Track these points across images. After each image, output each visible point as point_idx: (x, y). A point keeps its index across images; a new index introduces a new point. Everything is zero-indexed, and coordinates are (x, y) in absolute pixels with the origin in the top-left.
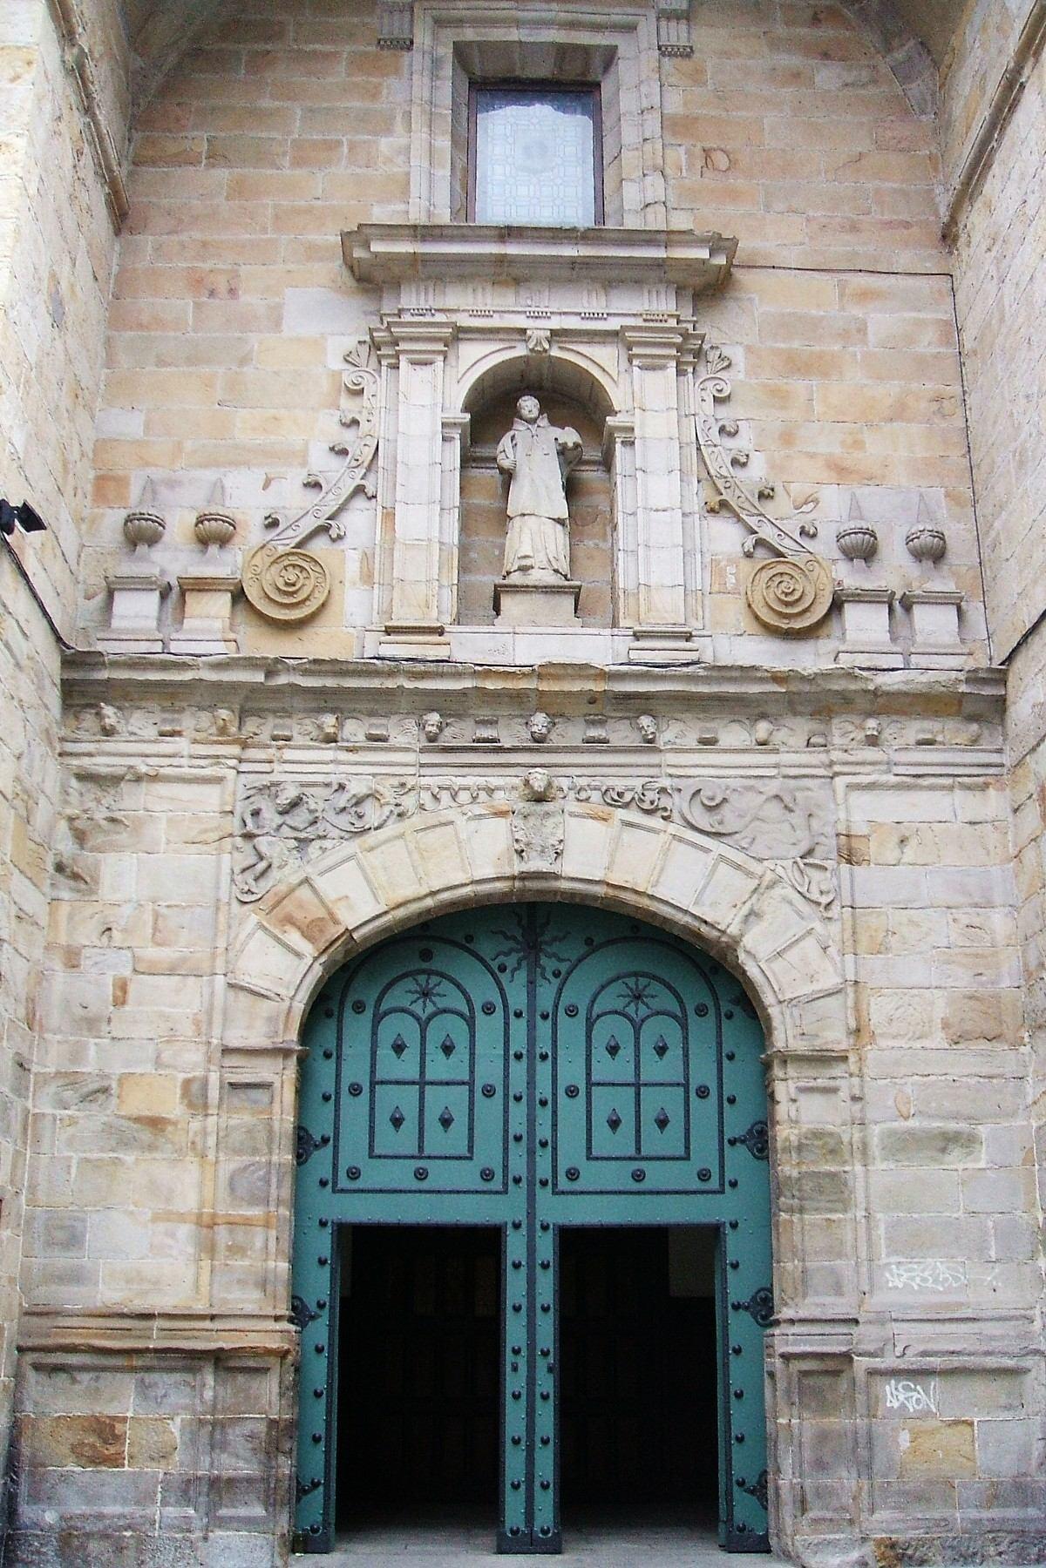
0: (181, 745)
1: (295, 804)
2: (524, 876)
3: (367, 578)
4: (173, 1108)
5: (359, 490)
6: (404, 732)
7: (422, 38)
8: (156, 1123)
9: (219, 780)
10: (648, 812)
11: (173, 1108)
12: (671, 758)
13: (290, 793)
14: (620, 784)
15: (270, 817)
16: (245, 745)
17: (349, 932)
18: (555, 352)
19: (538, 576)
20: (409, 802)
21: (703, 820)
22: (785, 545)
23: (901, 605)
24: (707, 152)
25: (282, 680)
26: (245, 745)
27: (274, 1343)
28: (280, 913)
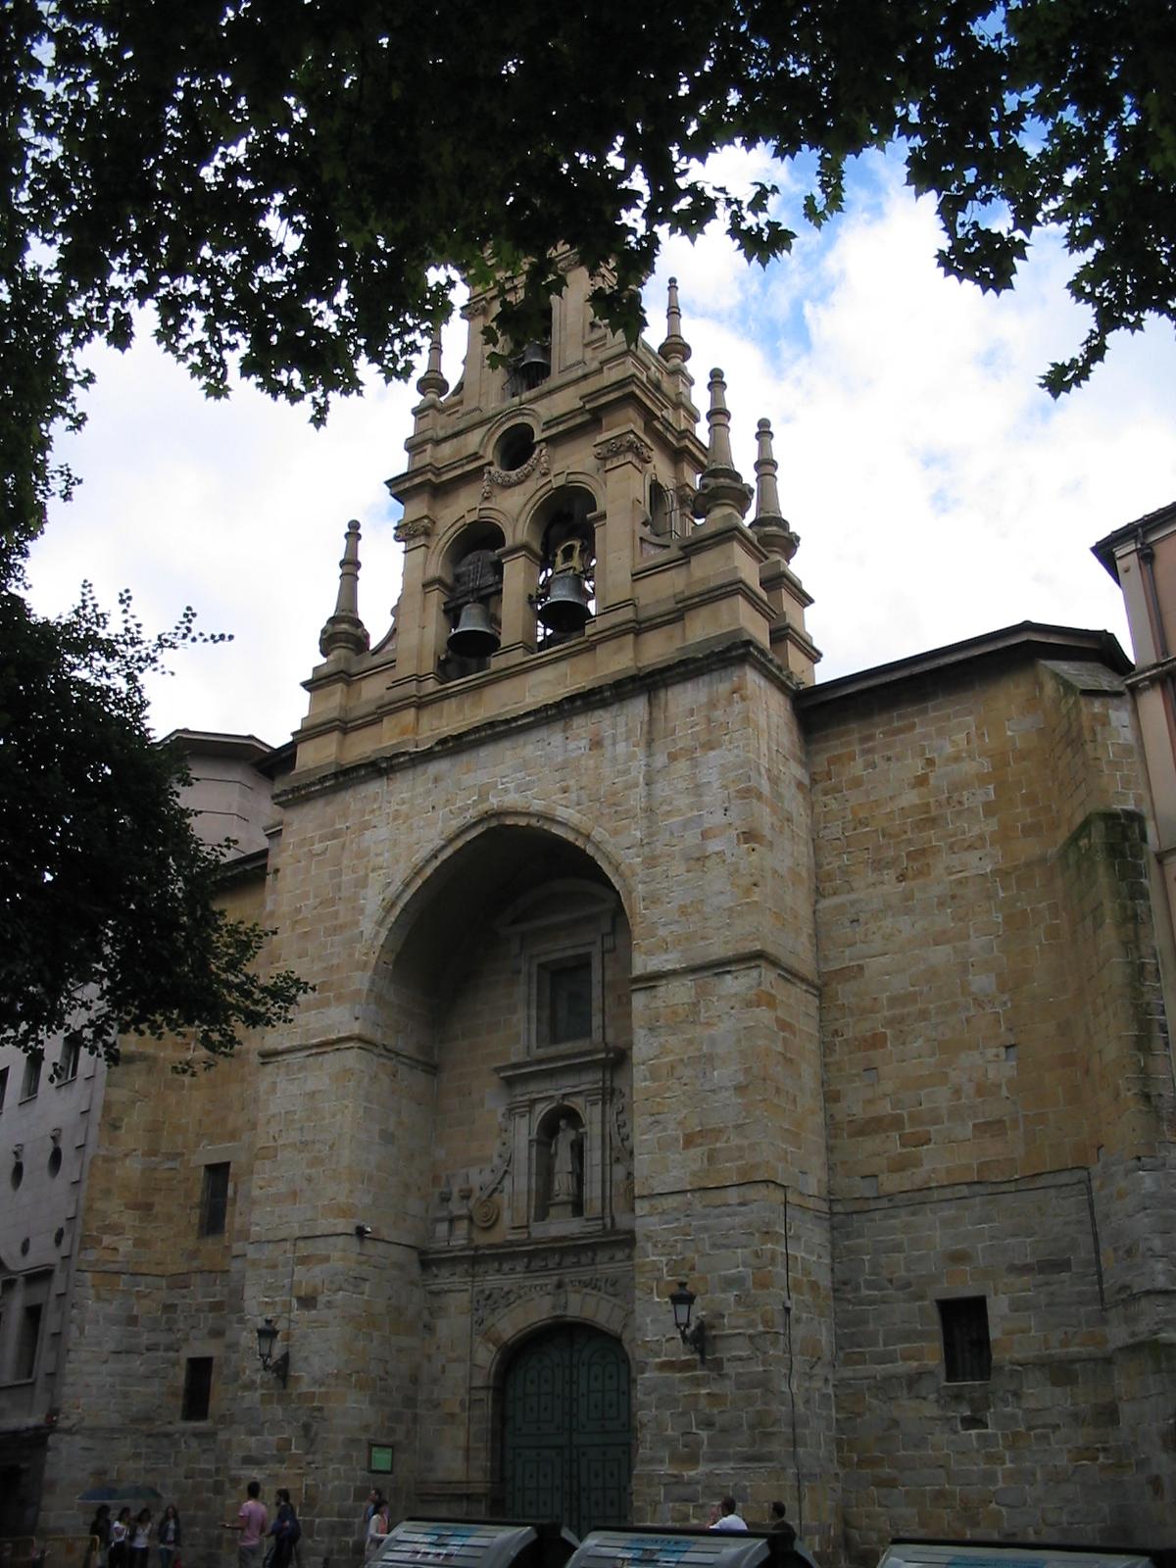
0: (455, 1279)
1: (490, 1296)
2: (557, 1317)
4: (457, 1410)
5: (506, 1172)
6: (520, 1266)
7: (524, 969)
8: (452, 1415)
9: (467, 1290)
10: (593, 1289)
11: (457, 1410)
12: (599, 1267)
13: (487, 1292)
14: (584, 1278)
15: (482, 1302)
16: (473, 1276)
17: (505, 1343)
18: (566, 1103)
20: (522, 1292)
21: (611, 1290)
24: (619, 997)
25: (481, 1252)
26: (473, 1276)
27: (481, 1491)
28: (487, 1336)
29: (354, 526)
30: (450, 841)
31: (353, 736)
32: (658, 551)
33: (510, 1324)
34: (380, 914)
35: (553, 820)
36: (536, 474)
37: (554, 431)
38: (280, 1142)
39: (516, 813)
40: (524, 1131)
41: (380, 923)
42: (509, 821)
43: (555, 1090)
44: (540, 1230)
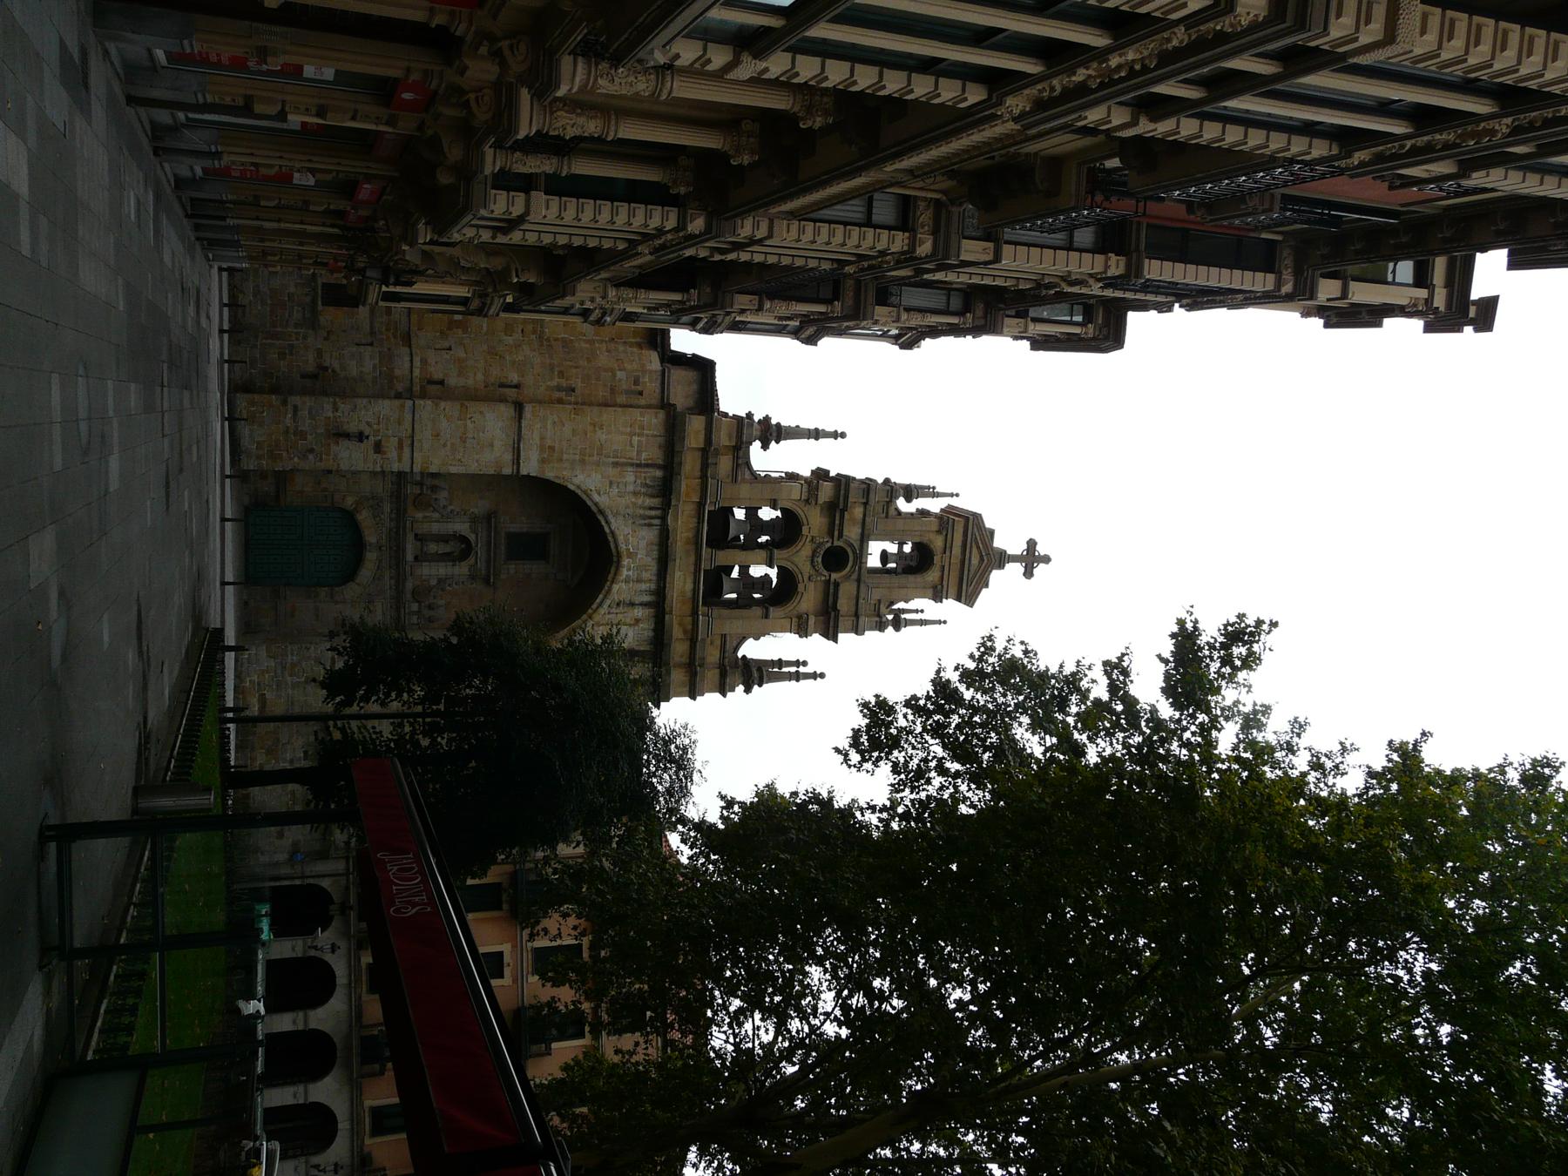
3: (425, 517)
8: (319, 483)
19: (425, 549)
22: (432, 594)
23: (419, 612)
29: (843, 435)
30: (612, 533)
31: (698, 455)
32: (735, 645)
33: (364, 517)
34: (583, 487)
35: (605, 596)
36: (813, 572)
37: (832, 587)
38: (469, 421)
39: (615, 574)
40: (462, 527)
41: (579, 487)
42: (613, 570)
43: (480, 551)
44: (410, 537)
